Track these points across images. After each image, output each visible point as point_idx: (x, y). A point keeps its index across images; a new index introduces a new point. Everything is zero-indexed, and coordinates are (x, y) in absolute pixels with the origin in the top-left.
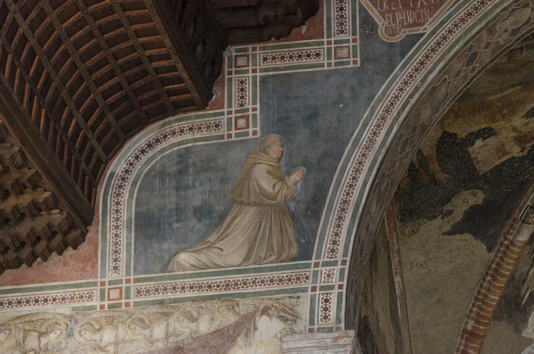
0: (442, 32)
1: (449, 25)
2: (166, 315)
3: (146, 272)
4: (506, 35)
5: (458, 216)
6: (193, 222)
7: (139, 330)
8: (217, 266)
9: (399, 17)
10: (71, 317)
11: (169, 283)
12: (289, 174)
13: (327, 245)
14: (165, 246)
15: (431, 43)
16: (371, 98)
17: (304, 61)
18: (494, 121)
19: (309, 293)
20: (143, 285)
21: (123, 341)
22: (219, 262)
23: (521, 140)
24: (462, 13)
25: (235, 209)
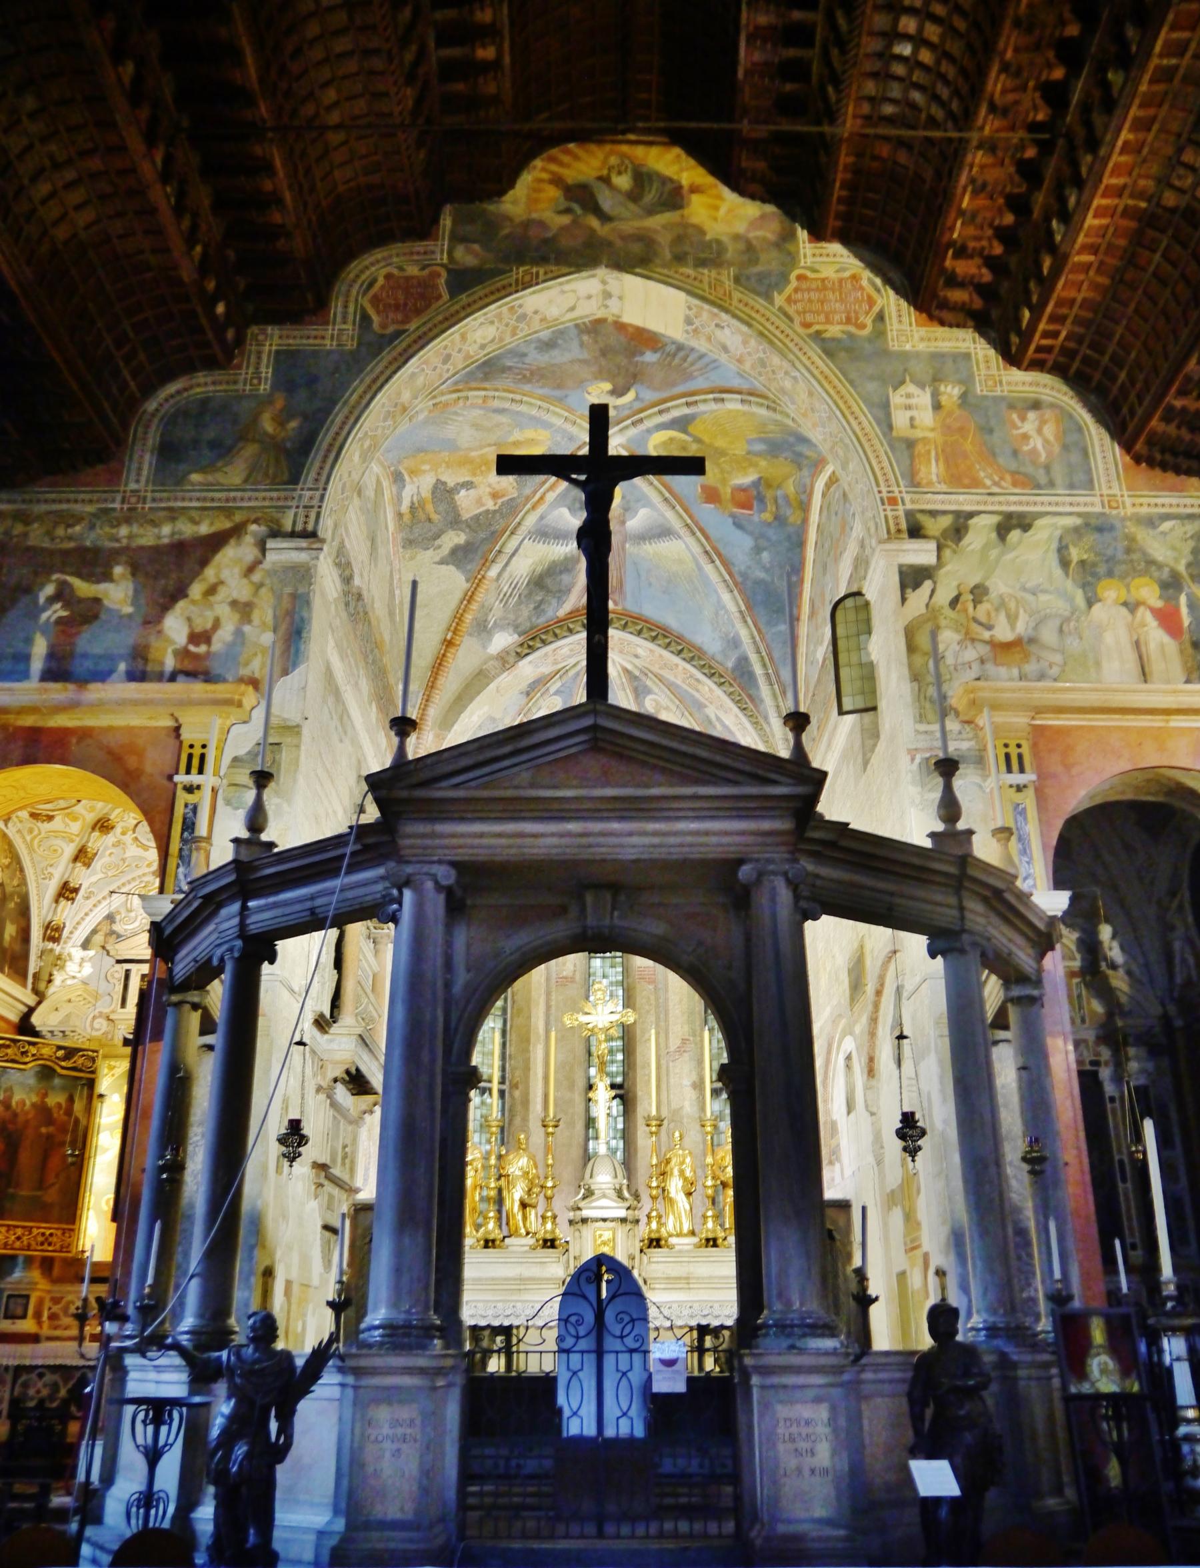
0: (424, 329)
1: (429, 325)
2: (173, 519)
3: (163, 484)
4: (476, 347)
5: (445, 550)
6: (206, 452)
7: (149, 528)
8: (219, 484)
9: (391, 315)
10: (94, 515)
11: (180, 494)
12: (288, 421)
13: (313, 475)
14: (183, 467)
15: (414, 337)
16: (361, 371)
17: (311, 341)
18: (474, 475)
19: (293, 511)
20: (158, 495)
21: (136, 536)
22: (222, 480)
23: (495, 496)
24: (440, 318)
25: (240, 445)
